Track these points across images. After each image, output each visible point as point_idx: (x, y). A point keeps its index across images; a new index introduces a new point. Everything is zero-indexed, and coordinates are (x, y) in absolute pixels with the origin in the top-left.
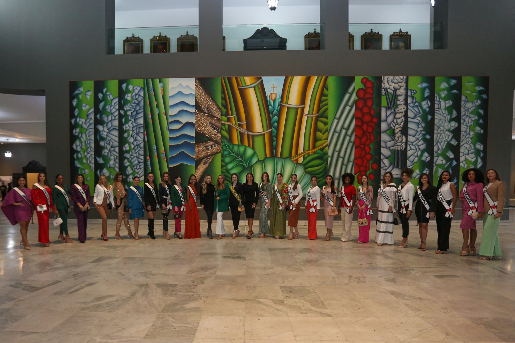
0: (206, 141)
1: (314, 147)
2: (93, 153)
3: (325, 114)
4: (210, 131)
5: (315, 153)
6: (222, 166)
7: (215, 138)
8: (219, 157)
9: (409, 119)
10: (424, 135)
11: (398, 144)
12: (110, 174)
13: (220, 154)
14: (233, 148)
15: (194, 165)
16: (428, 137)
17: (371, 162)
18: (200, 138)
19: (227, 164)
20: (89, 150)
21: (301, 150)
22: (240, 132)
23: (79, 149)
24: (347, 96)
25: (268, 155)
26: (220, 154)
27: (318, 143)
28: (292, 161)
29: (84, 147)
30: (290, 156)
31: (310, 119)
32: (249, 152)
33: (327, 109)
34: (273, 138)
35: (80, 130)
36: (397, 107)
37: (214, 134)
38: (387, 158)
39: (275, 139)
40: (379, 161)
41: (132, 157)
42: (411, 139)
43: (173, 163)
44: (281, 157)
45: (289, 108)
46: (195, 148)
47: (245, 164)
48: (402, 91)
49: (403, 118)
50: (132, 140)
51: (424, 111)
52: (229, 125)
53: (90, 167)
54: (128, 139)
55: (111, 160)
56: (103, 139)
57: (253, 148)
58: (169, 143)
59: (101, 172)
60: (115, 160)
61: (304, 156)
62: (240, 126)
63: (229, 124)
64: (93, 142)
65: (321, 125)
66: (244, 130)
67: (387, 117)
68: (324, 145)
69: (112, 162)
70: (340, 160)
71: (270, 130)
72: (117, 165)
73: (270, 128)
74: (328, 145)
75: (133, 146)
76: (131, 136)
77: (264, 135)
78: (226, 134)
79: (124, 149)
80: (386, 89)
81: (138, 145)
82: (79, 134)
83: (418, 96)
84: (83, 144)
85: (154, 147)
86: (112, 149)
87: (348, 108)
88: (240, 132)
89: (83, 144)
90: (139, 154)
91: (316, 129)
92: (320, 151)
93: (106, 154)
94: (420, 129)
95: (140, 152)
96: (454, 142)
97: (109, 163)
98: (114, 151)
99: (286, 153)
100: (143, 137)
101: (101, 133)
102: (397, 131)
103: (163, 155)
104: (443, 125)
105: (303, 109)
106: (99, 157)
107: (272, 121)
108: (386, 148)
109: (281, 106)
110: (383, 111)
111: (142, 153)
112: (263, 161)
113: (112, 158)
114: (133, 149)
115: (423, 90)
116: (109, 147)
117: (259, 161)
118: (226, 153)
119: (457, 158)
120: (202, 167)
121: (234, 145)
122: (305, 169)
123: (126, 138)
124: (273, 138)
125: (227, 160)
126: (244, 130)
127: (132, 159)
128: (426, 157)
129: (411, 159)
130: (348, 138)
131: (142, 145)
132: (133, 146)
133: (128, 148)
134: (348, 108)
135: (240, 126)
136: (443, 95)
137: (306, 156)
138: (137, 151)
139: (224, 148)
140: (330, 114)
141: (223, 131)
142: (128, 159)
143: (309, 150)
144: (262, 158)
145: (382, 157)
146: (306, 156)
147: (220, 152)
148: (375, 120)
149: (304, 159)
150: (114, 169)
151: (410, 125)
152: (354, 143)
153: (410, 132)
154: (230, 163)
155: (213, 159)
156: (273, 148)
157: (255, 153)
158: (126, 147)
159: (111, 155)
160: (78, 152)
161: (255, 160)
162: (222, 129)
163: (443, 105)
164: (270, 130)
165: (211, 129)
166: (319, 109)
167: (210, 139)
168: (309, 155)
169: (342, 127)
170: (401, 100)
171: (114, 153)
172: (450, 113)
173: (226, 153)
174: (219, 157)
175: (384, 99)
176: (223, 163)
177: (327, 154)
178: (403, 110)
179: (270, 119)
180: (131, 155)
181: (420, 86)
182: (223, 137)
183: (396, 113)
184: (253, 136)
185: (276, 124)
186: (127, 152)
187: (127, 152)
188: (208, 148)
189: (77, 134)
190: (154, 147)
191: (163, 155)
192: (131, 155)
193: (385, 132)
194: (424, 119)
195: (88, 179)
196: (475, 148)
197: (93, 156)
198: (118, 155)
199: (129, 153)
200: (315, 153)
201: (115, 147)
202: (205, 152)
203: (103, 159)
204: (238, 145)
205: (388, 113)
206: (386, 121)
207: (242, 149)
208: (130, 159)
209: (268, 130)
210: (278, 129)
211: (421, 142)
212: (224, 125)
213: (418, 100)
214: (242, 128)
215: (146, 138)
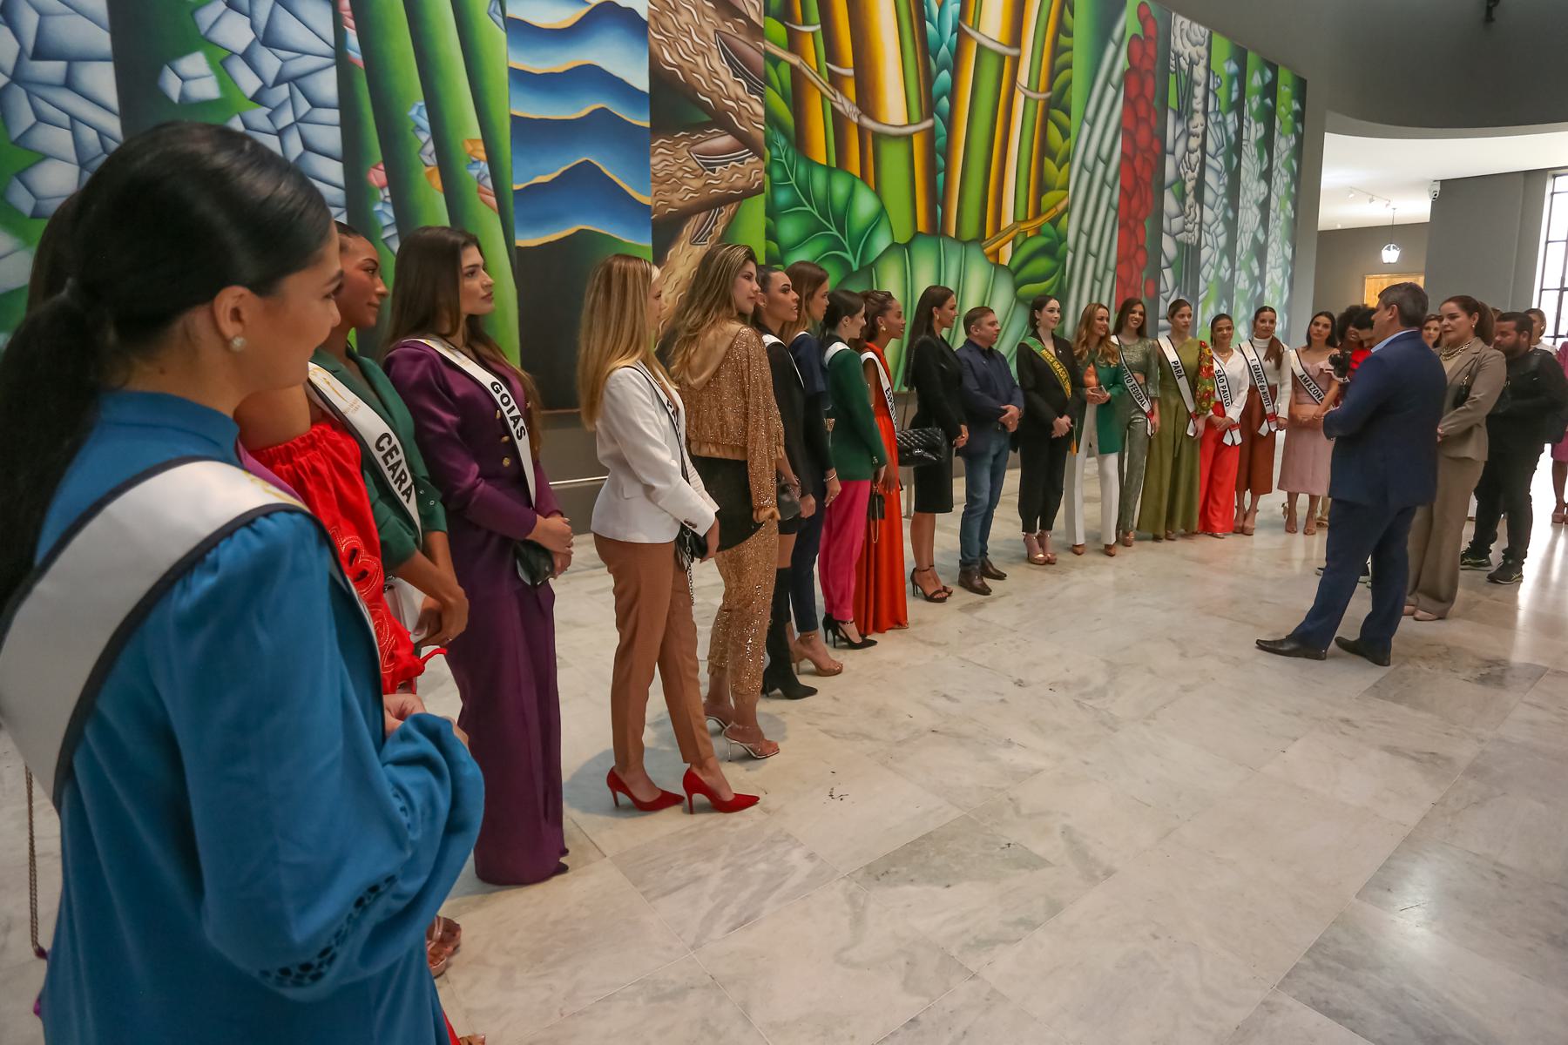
0: (702, 127)
1: (1038, 213)
3: (1066, 98)
4: (716, 77)
5: (1039, 232)
7: (738, 115)
9: (1208, 159)
10: (1226, 208)
11: (1190, 226)
14: (809, 175)
16: (1230, 214)
17: (1144, 275)
18: (674, 105)
21: (1008, 220)
22: (834, 109)
24: (1111, 49)
25: (921, 227)
26: (758, 205)
27: (1048, 198)
28: (986, 256)
30: (980, 239)
31: (1031, 105)
32: (865, 204)
33: (1069, 83)
34: (937, 153)
36: (1191, 118)
37: (737, 100)
38: (1170, 265)
39: (941, 161)
40: (1157, 272)
42: (1208, 215)
43: (537, 222)
44: (958, 238)
45: (980, 47)
46: (644, 153)
47: (849, 257)
48: (1199, 73)
49: (1198, 153)
51: (1228, 139)
52: (793, 68)
57: (877, 192)
58: (511, 105)
61: (1014, 239)
62: (835, 80)
63: (795, 60)
65: (1054, 133)
66: (847, 106)
67: (1175, 141)
68: (1061, 207)
70: (1091, 260)
71: (928, 123)
73: (930, 116)
74: (1068, 210)
77: (909, 137)
78: (783, 110)
80: (1178, 55)
83: (1222, 93)
85: (416, 113)
87: (1111, 91)
88: (834, 109)
90: (308, 146)
91: (1045, 150)
92: (1048, 228)
94: (1222, 191)
95: (308, 129)
96: (1261, 237)
99: (970, 230)
100: (330, 35)
102: (1190, 185)
103: (476, 172)
104: (1252, 189)
105: (1016, 61)
107: (936, 89)
108: (1169, 234)
109: (958, 29)
110: (1171, 117)
111: (329, 136)
112: (908, 245)
115: (1231, 78)
117: (894, 246)
118: (783, 197)
119: (1262, 278)
121: (811, 163)
122: (1017, 287)
124: (937, 153)
125: (789, 229)
126: (847, 106)
128: (1225, 273)
129: (1205, 272)
130: (1107, 191)
131: (327, 85)
134: (1111, 91)
135: (835, 80)
136: (1255, 106)
137: (1020, 240)
138: (286, 118)
139: (777, 173)
140: (1076, 96)
141: (769, 91)
143: (1026, 220)
144: (903, 236)
145: (1164, 263)
146: (1020, 240)
148: (1156, 146)
149: (1015, 251)
151: (1210, 177)
152: (1118, 210)
153: (1208, 196)
154: (799, 243)
155: (731, 221)
156: (936, 198)
157: (882, 212)
161: (881, 242)
162: (768, 81)
163: (1255, 131)
164: (928, 123)
165: (722, 67)
166: (1053, 75)
167: (720, 120)
168: (1026, 239)
169: (1098, 155)
170: (1199, 91)
172: (1261, 158)
175: (1172, 78)
176: (774, 246)
177: (1063, 238)
178: (1200, 130)
179: (928, 78)
181: (1226, 66)
182: (772, 119)
183: (1189, 135)
184: (877, 136)
185: (945, 101)
188: (709, 162)
190: (416, 113)
191: (476, 172)
193: (1170, 186)
194: (1228, 162)
196: (1284, 256)
200: (1039, 232)
202: (697, 184)
204: (829, 170)
205: (1178, 132)
206: (1173, 153)
207: (840, 188)
209: (922, 120)
210: (950, 122)
211: (1221, 228)
212: (775, 61)
213: (1223, 106)
214: (842, 92)
215: (353, 38)
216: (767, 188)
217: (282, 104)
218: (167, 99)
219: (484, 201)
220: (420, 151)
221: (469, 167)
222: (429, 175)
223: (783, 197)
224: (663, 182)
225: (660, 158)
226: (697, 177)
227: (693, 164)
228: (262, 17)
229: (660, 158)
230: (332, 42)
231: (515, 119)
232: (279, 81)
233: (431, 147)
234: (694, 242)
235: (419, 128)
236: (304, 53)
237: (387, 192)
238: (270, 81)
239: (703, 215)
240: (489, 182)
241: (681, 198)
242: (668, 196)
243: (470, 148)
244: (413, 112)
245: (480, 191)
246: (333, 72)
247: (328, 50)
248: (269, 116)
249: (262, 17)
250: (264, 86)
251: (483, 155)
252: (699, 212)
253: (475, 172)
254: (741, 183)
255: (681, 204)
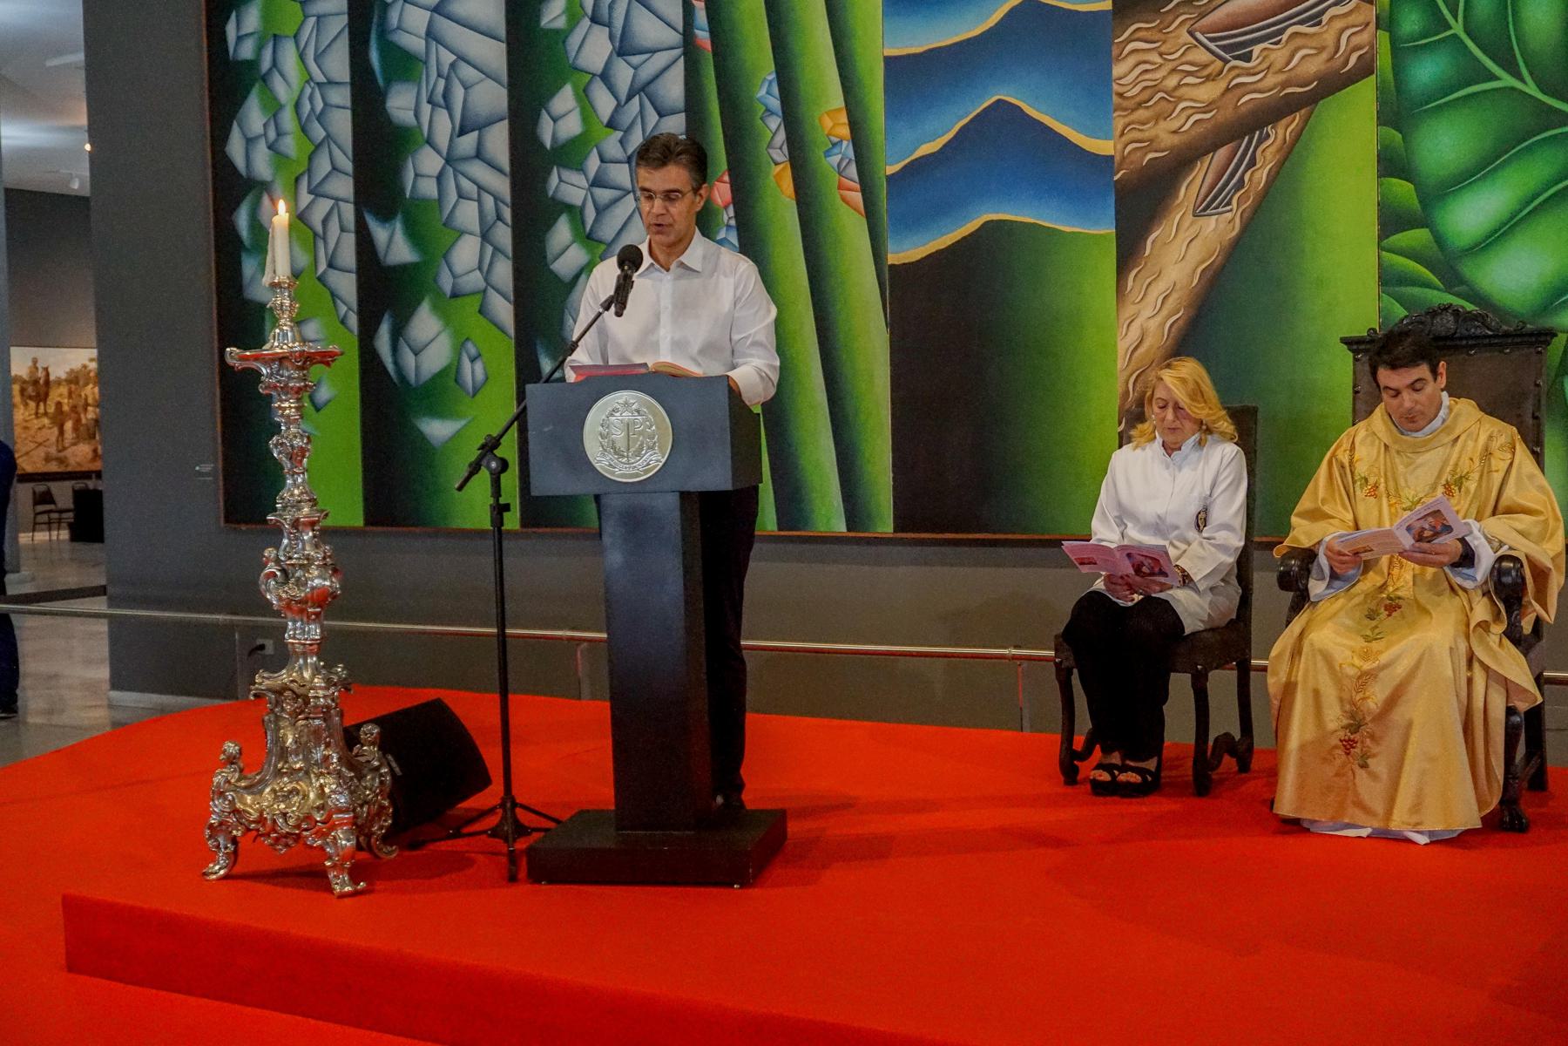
2: (344, 187)
6: (1391, 221)
8: (1352, 125)
12: (460, 347)
13: (1363, 98)
15: (1108, 230)
19: (1436, 194)
20: (323, 166)
23: (262, 166)
26: (1363, 98)
29: (290, 145)
35: (267, 17)
41: (605, 195)
43: (912, 222)
50: (594, 49)
53: (334, 295)
54: (574, 41)
55: (462, 233)
56: (404, 65)
59: (397, 334)
60: (485, 236)
64: (342, 96)
69: (466, 253)
72: (504, 272)
75: (605, 104)
76: (595, 20)
79: (546, 132)
81: (642, 89)
82: (260, 49)
84: (288, 119)
85: (764, 92)
86: (468, 143)
89: (288, 119)
93: (429, 188)
97: (446, 256)
98: (479, 155)
101: (393, 17)
106: (386, 217)
113: (468, 215)
114: (612, 124)
116: (443, 127)
120: (1186, 245)
123: (561, 36)
125: (1444, 144)
127: (601, 211)
132: (605, 104)
133: (571, 126)
142: (575, 213)
147: (1366, 68)
150: (483, 311)
155: (1289, 152)
158: (562, 118)
159: (461, 196)
160: (263, 187)
171: (478, 170)
173: (1426, 71)
174: (1352, 125)
176: (1403, 190)
180: (598, 182)
186: (569, 154)
187: (569, 154)
189: (247, 51)
190: (764, 92)
192: (598, 182)
195: (324, 394)
197: (349, 211)
198: (502, 186)
199: (581, 169)
201: (482, 126)
203: (415, 235)
208: (590, 214)
215: (701, 16)
216: (1384, 60)
217: (633, 123)
218: (542, 146)
219: (844, 199)
220: (770, 146)
221: (827, 154)
222: (778, 177)
223: (1426, 71)
224: (1139, 105)
225: (1132, 60)
226: (1208, 78)
227: (1201, 56)
228: (619, 23)
229: (1132, 60)
230: (681, 29)
231: (890, 62)
232: (630, 98)
233: (781, 136)
234: (1202, 210)
235: (769, 111)
236: (653, 51)
237: (731, 211)
238: (623, 98)
239: (1222, 153)
240: (853, 171)
241: (1168, 133)
242: (1149, 131)
243: (828, 123)
244: (763, 92)
245: (840, 187)
246: (679, 70)
247: (675, 38)
248: (621, 142)
249: (619, 23)
250: (619, 107)
251: (845, 131)
252: (1215, 147)
253: (835, 159)
254: (1315, 66)
255: (1176, 139)
